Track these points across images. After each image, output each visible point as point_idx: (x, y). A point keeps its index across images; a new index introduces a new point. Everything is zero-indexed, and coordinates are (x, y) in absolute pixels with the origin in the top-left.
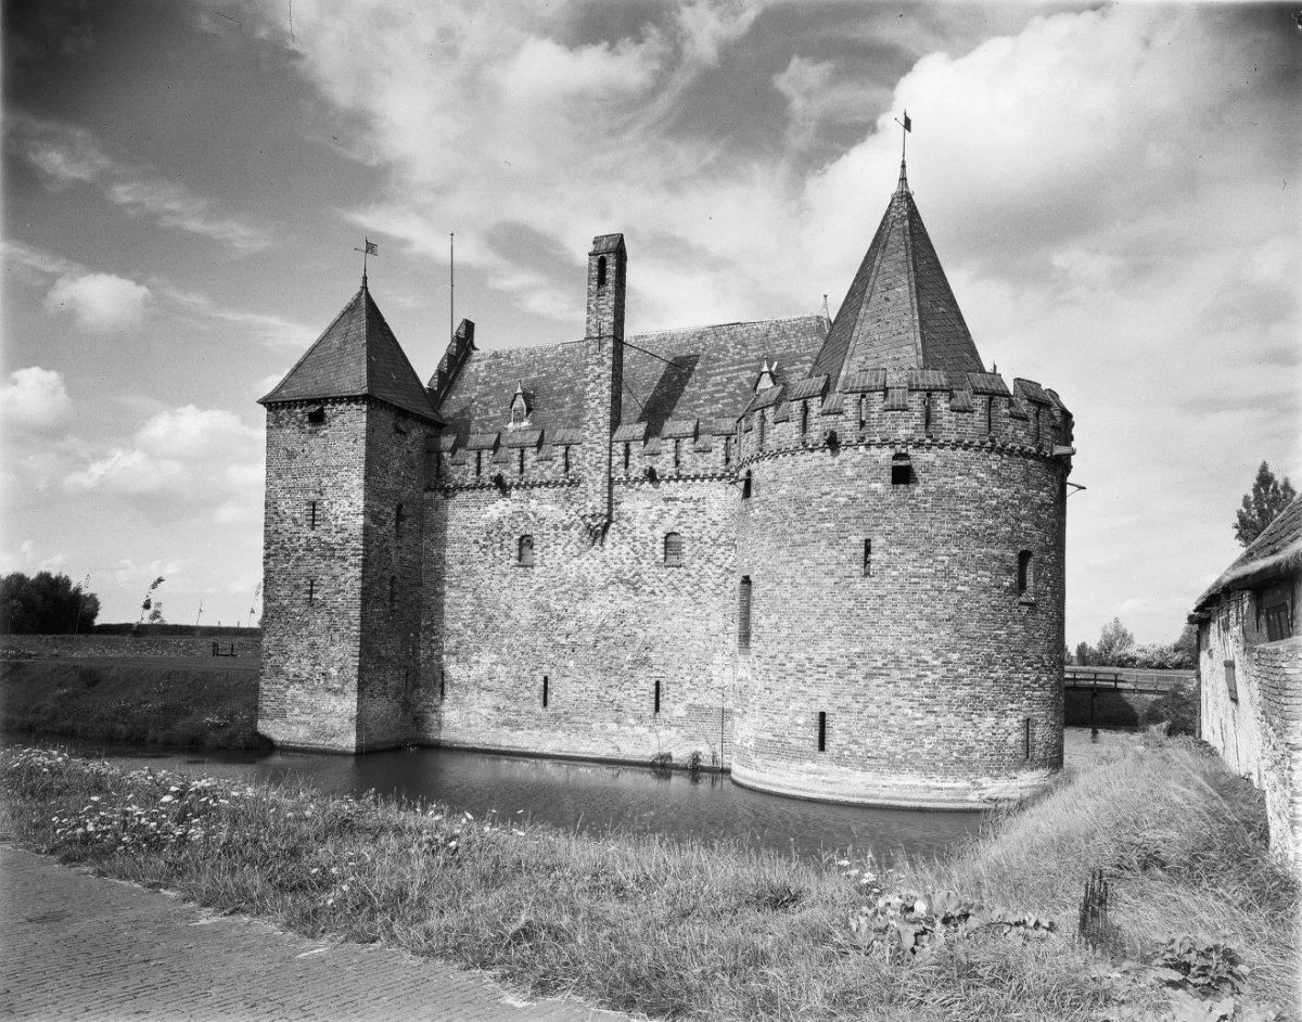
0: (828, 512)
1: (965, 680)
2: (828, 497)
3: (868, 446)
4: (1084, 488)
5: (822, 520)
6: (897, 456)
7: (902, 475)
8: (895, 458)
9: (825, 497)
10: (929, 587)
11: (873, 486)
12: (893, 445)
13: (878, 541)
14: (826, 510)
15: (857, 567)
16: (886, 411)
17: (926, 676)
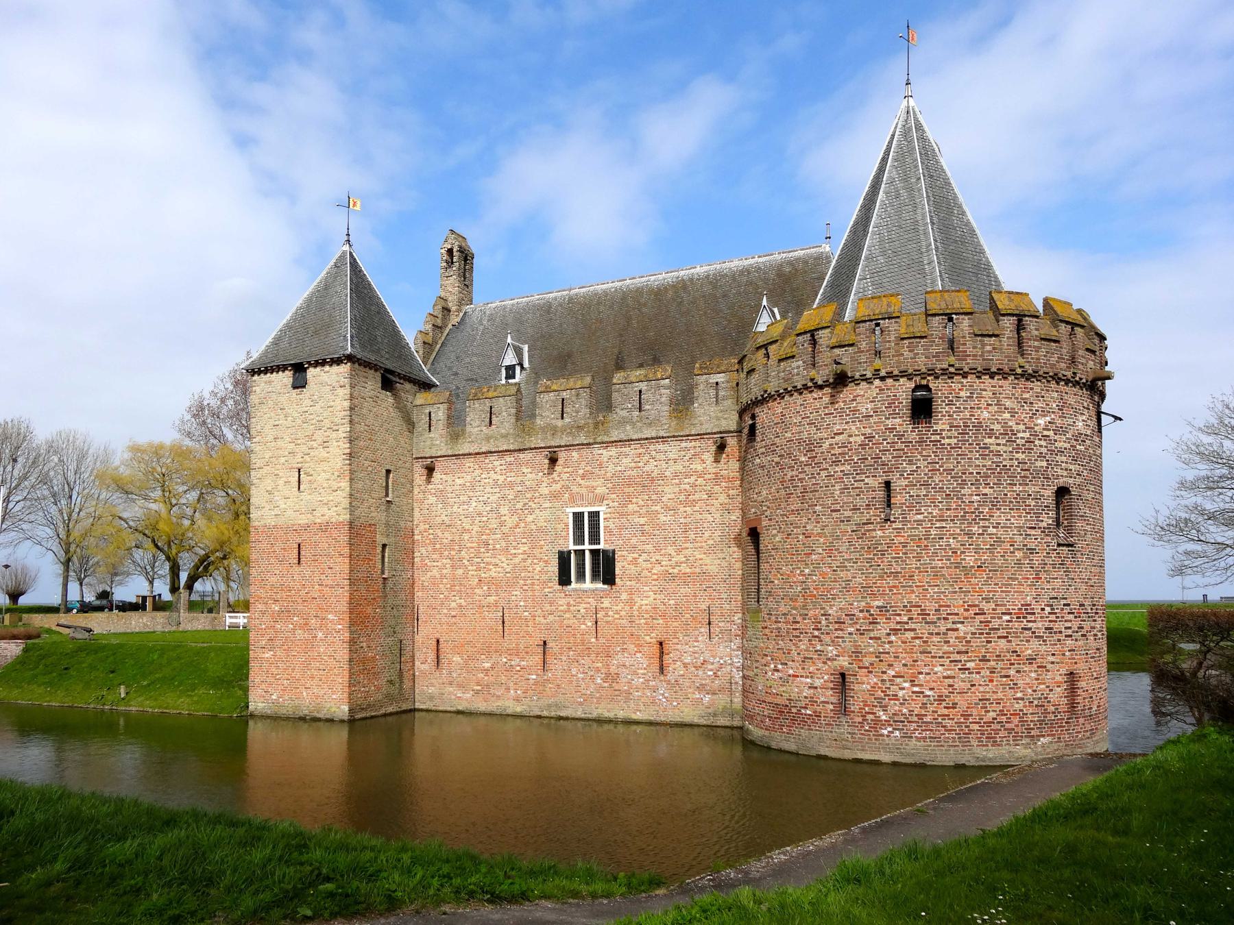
0: (843, 454)
1: (1000, 633)
2: (841, 437)
3: (883, 379)
4: (1120, 419)
5: (836, 463)
6: (918, 387)
7: (922, 409)
8: (914, 391)
9: (838, 438)
10: (958, 531)
11: (889, 423)
12: (910, 377)
13: (898, 483)
14: (840, 451)
15: (875, 514)
16: (903, 339)
17: (957, 630)
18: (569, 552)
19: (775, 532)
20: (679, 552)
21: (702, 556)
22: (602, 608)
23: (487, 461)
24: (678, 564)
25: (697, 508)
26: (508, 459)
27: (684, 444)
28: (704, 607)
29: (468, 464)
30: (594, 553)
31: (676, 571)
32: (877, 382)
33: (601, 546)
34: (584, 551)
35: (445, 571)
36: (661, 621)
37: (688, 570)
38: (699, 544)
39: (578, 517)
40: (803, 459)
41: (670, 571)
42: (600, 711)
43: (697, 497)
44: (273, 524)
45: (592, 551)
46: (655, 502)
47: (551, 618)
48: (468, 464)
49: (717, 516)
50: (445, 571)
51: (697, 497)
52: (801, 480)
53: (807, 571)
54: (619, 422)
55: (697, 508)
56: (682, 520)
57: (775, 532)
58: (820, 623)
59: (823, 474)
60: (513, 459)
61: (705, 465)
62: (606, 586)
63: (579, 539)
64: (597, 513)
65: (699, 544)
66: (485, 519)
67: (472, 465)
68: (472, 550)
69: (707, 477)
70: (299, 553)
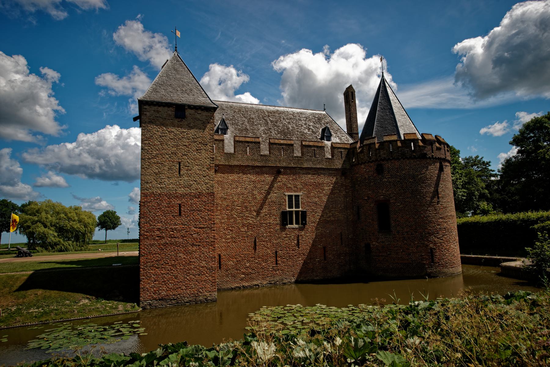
18: (287, 212)
19: (398, 204)
20: (330, 212)
21: (338, 214)
22: (301, 235)
23: (246, 170)
24: (330, 217)
25: (336, 196)
26: (257, 170)
27: (330, 172)
28: (339, 233)
29: (236, 170)
30: (297, 212)
31: (329, 219)
32: (432, 160)
33: (300, 209)
34: (292, 211)
35: (223, 221)
36: (324, 239)
37: (333, 219)
38: (337, 209)
39: (290, 197)
40: (411, 180)
41: (327, 219)
42: (302, 278)
43: (336, 191)
44: (159, 192)
45: (296, 211)
46: (321, 193)
47: (279, 240)
48: (236, 170)
49: (342, 199)
50: (223, 221)
51: (336, 191)
52: (411, 187)
53: (416, 217)
54: (306, 160)
55: (336, 196)
56: (331, 200)
57: (398, 204)
58: (422, 234)
59: (419, 186)
60: (259, 170)
61: (338, 180)
62: (302, 226)
63: (290, 206)
64: (297, 197)
65: (337, 209)
66: (245, 196)
67: (238, 171)
68: (239, 211)
69: (338, 184)
70: (180, 210)
